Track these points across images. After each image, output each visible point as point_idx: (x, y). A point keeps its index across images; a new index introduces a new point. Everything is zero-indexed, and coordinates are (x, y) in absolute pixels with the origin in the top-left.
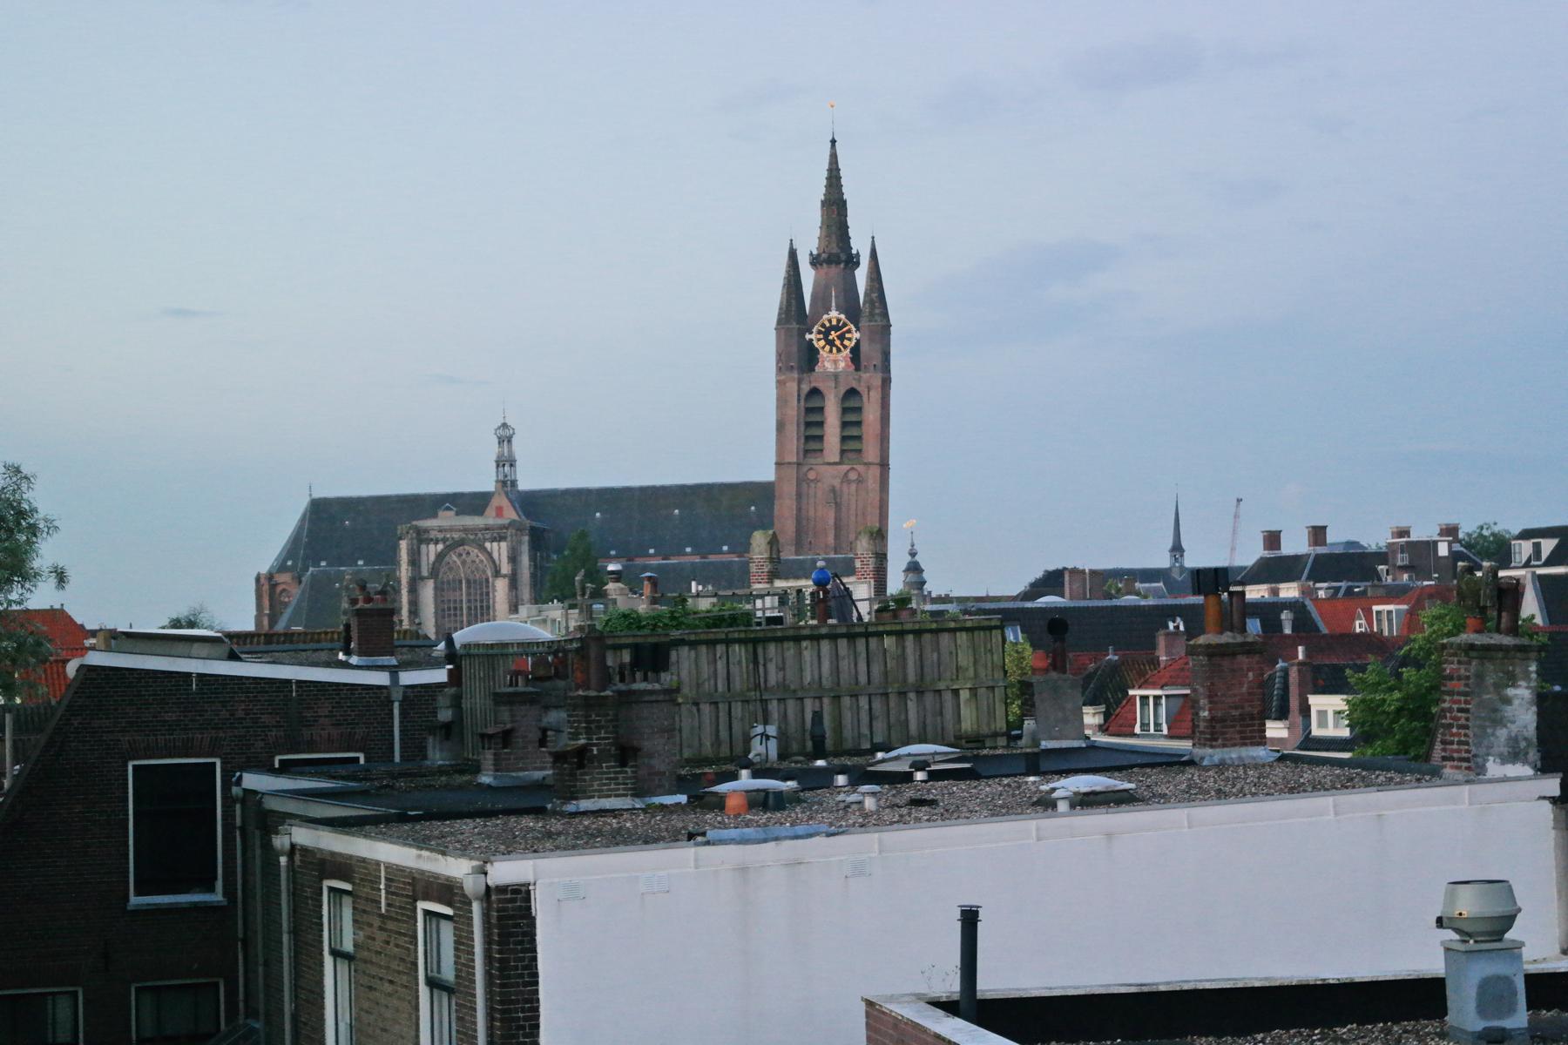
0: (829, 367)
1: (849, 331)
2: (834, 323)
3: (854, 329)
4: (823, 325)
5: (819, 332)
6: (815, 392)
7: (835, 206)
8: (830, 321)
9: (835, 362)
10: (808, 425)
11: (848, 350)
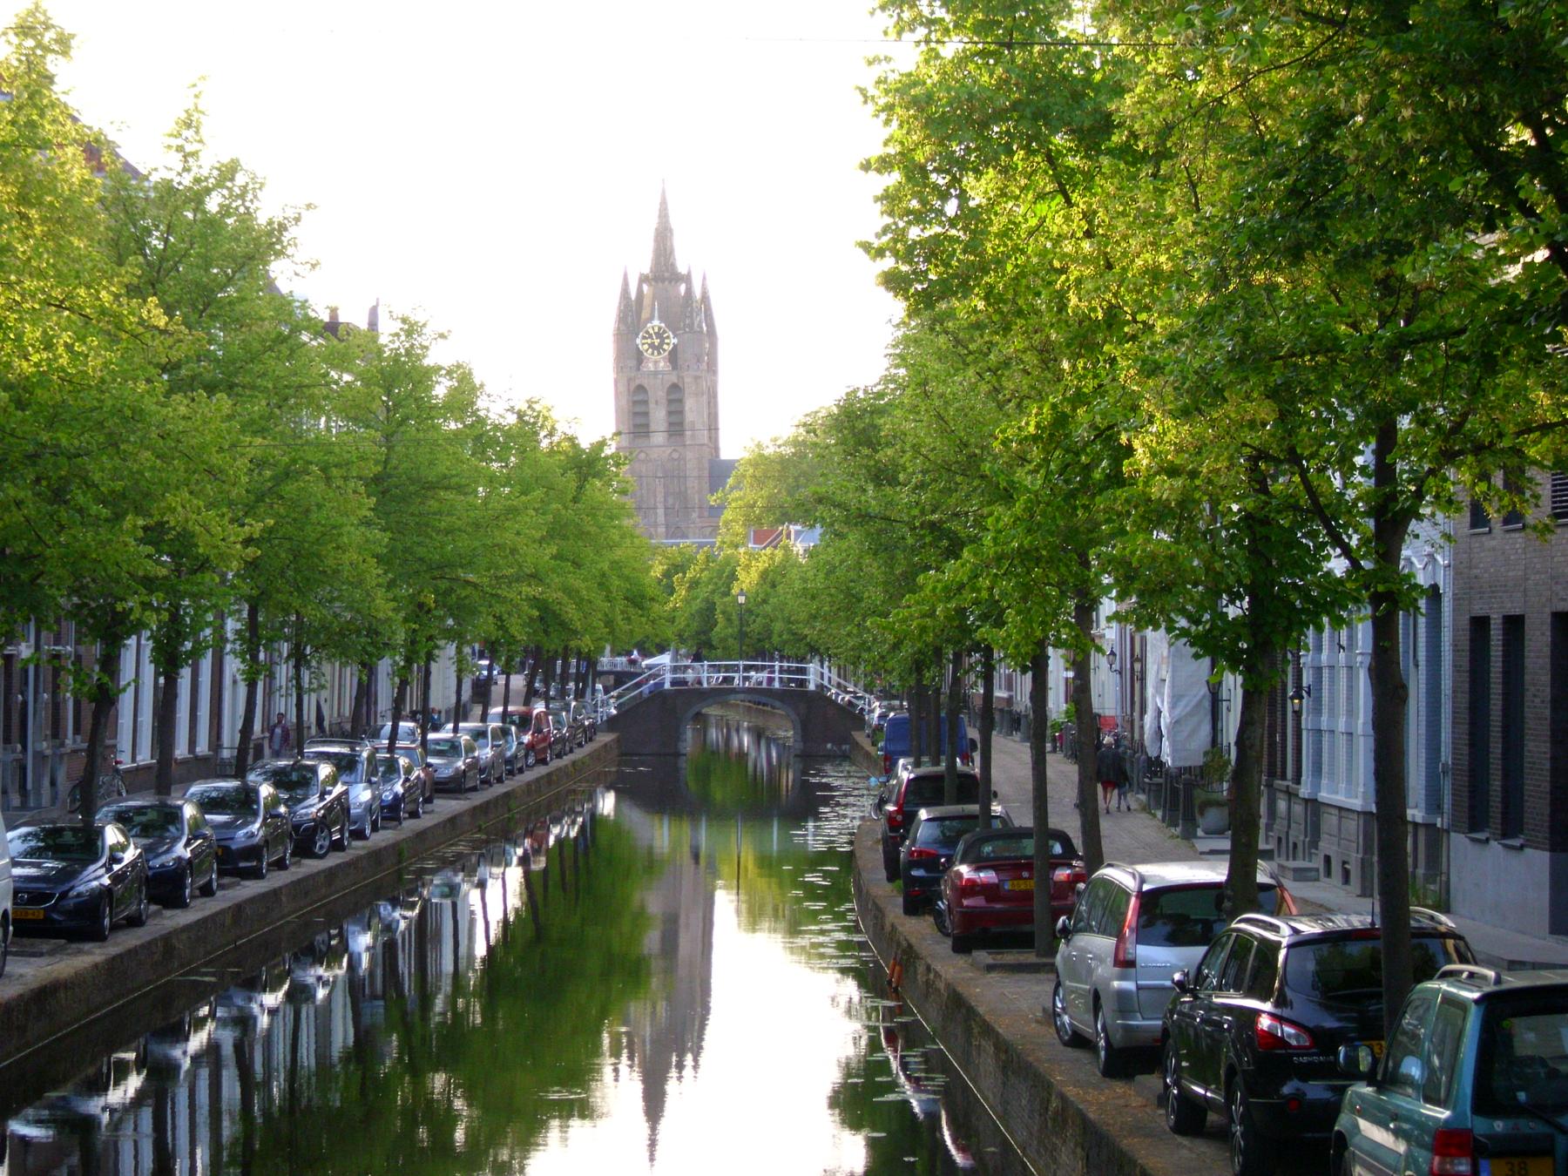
0: (651, 366)
1: (668, 337)
6: (641, 388)
7: (663, 238)
9: (656, 362)
10: (636, 414)
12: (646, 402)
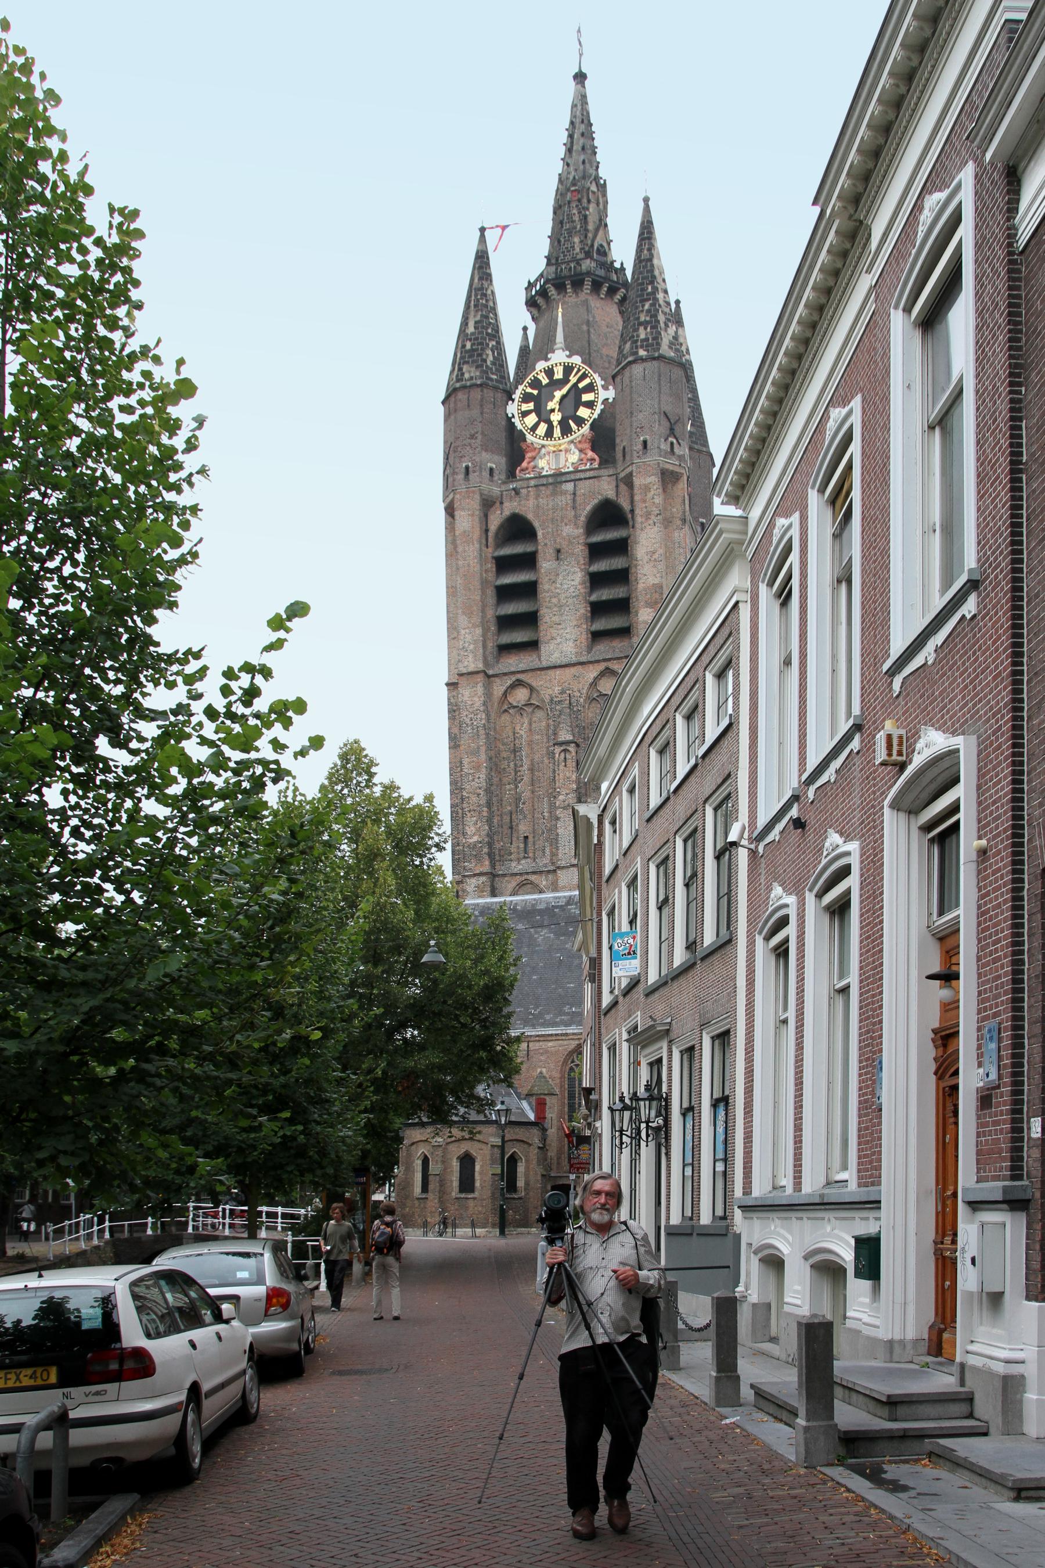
0: (545, 465)
1: (590, 388)
2: (559, 374)
3: (599, 382)
4: (536, 383)
5: (526, 398)
8: (549, 372)
10: (505, 593)
11: (586, 429)
12: (529, 561)
